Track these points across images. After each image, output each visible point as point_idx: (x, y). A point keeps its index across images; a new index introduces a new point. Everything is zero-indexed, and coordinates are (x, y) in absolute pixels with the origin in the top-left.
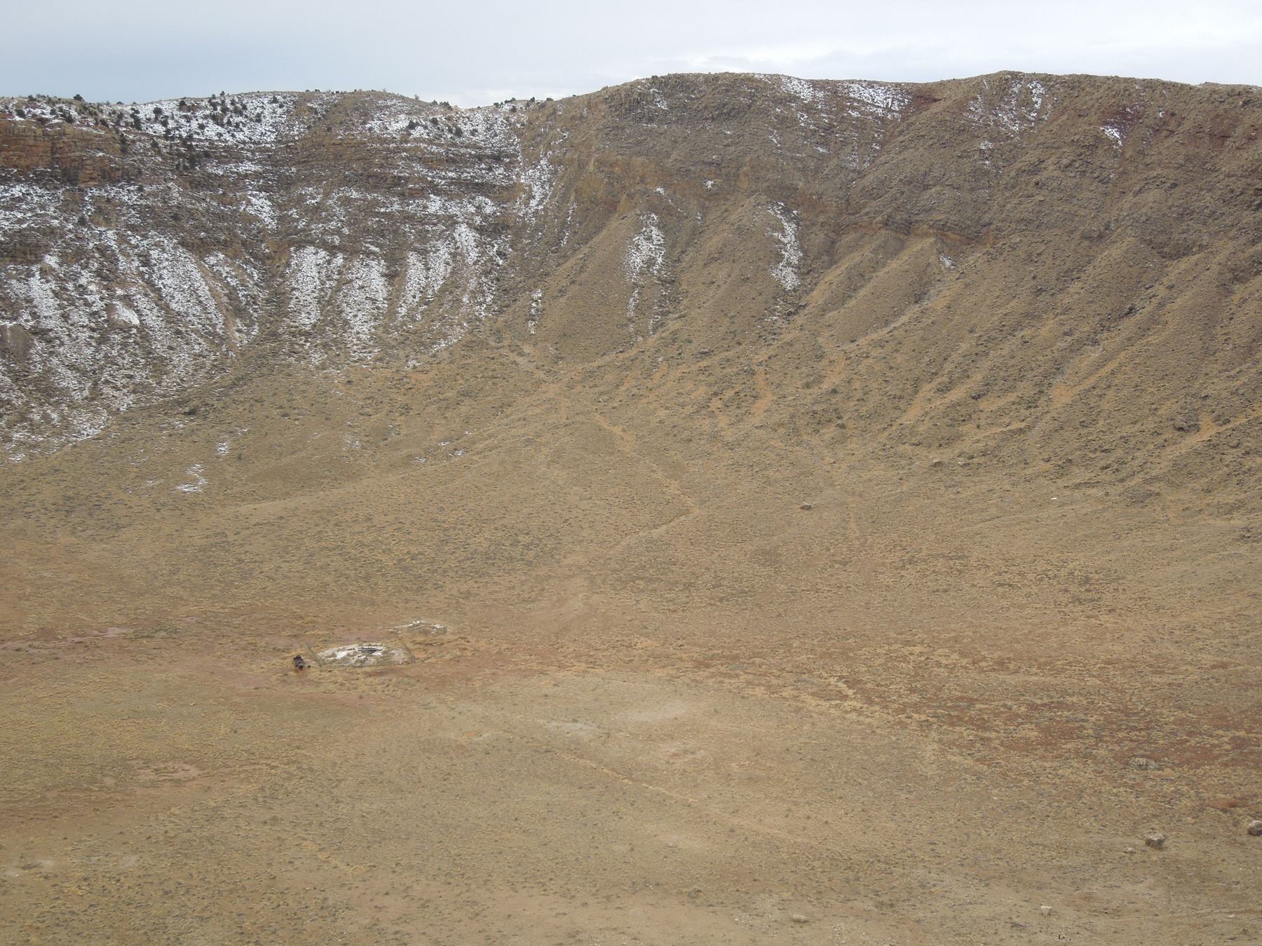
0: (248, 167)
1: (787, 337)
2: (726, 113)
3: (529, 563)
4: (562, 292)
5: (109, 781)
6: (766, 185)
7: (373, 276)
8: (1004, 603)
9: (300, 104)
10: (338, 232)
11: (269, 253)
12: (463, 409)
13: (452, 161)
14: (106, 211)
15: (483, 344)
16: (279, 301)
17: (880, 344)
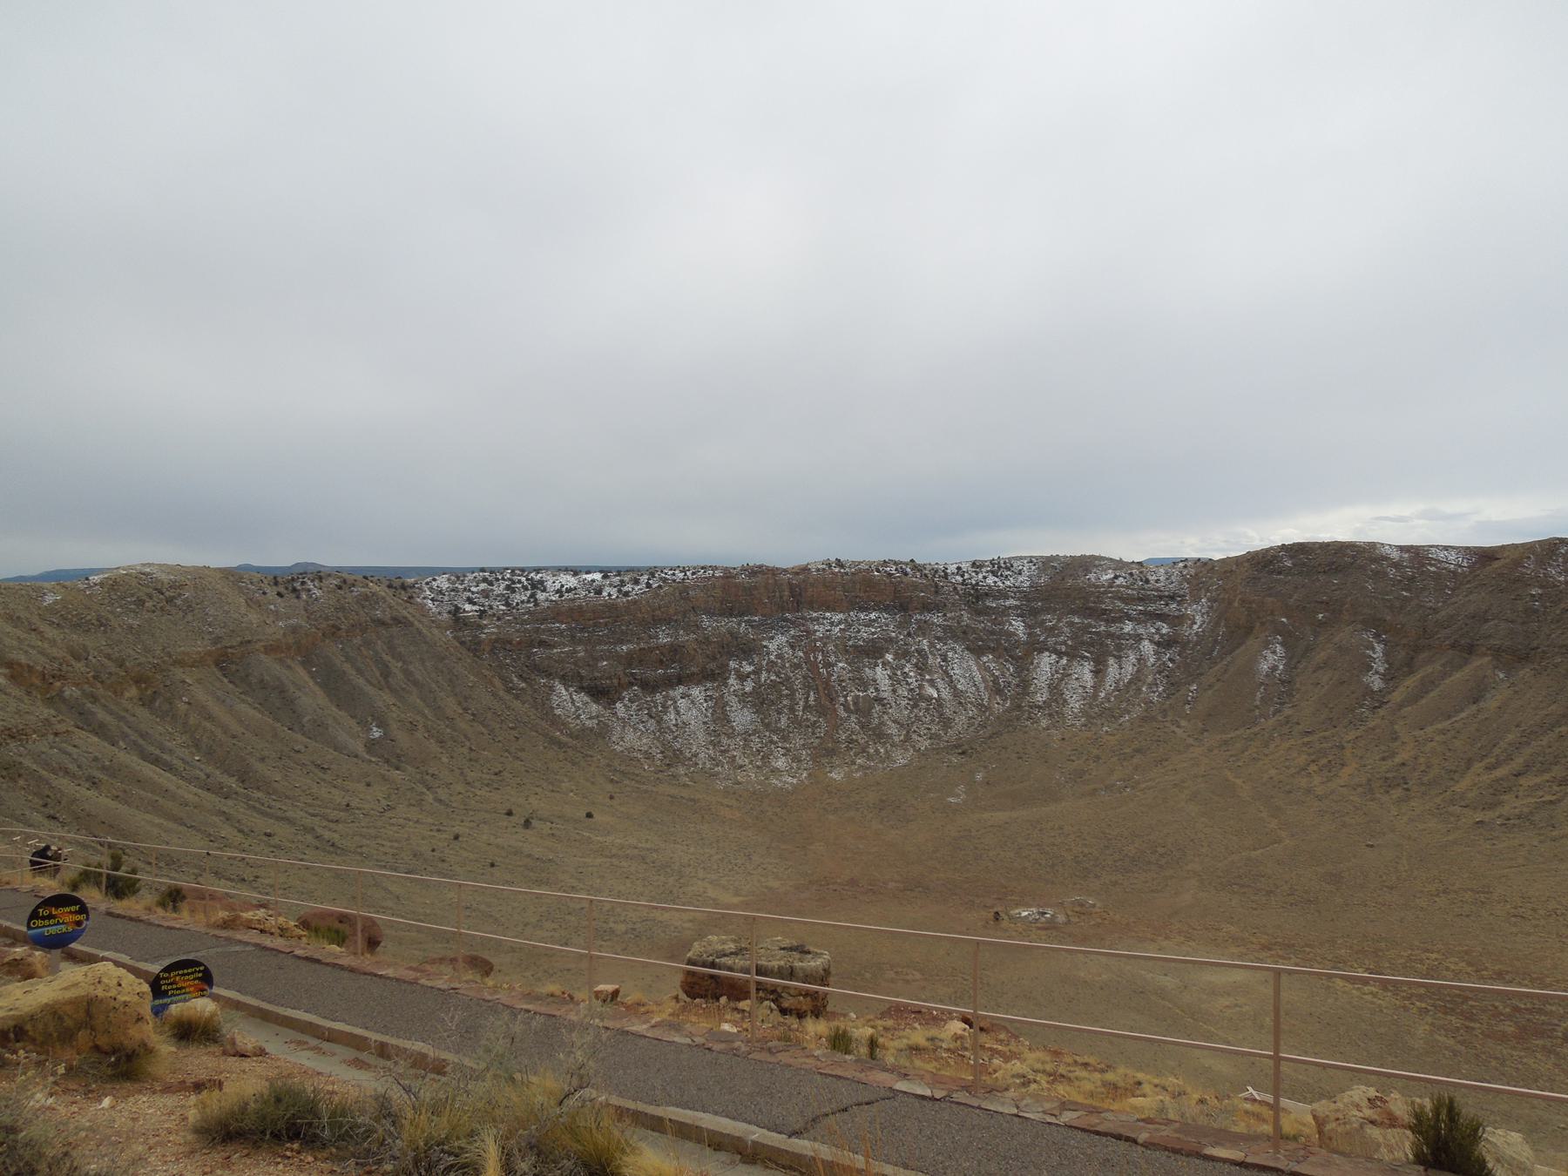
0: (1011, 602)
1: (1371, 724)
3: (1161, 867)
4: (1210, 686)
5: (868, 975)
7: (1085, 672)
8: (1514, 930)
9: (1046, 563)
10: (1064, 643)
11: (1021, 656)
12: (1135, 760)
13: (1141, 600)
14: (923, 629)
15: (1154, 718)
16: (1025, 685)
17: (1443, 732)
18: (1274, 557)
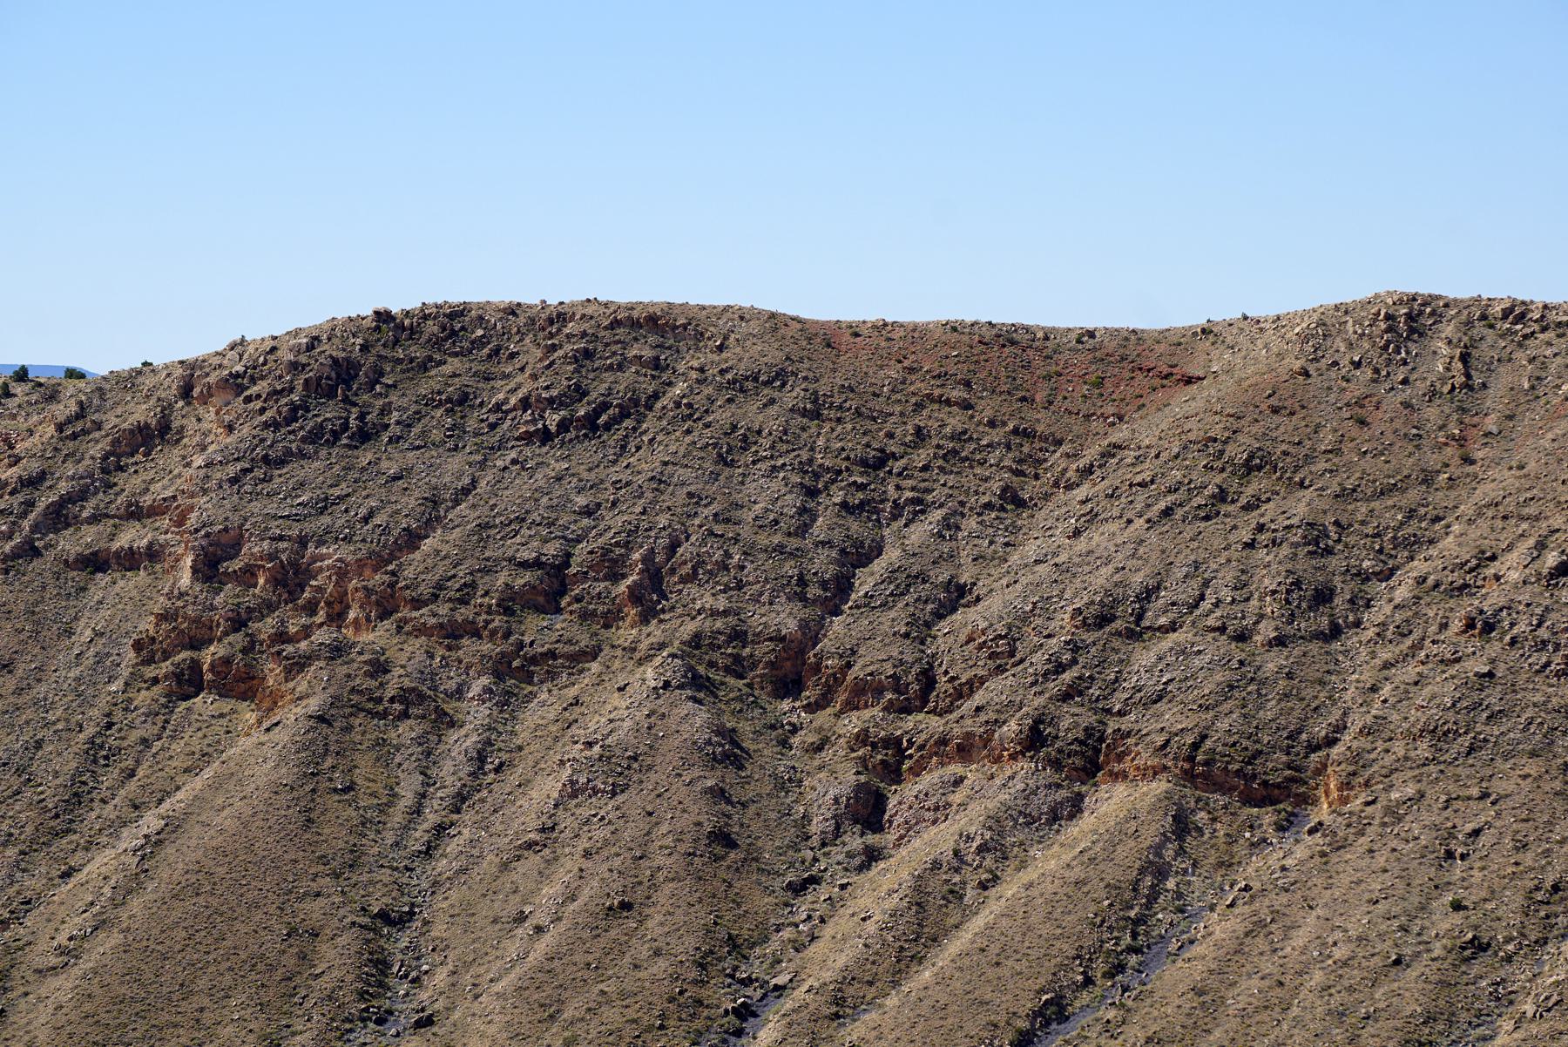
2: (588, 418)
6: (690, 627)
18: (344, 371)
